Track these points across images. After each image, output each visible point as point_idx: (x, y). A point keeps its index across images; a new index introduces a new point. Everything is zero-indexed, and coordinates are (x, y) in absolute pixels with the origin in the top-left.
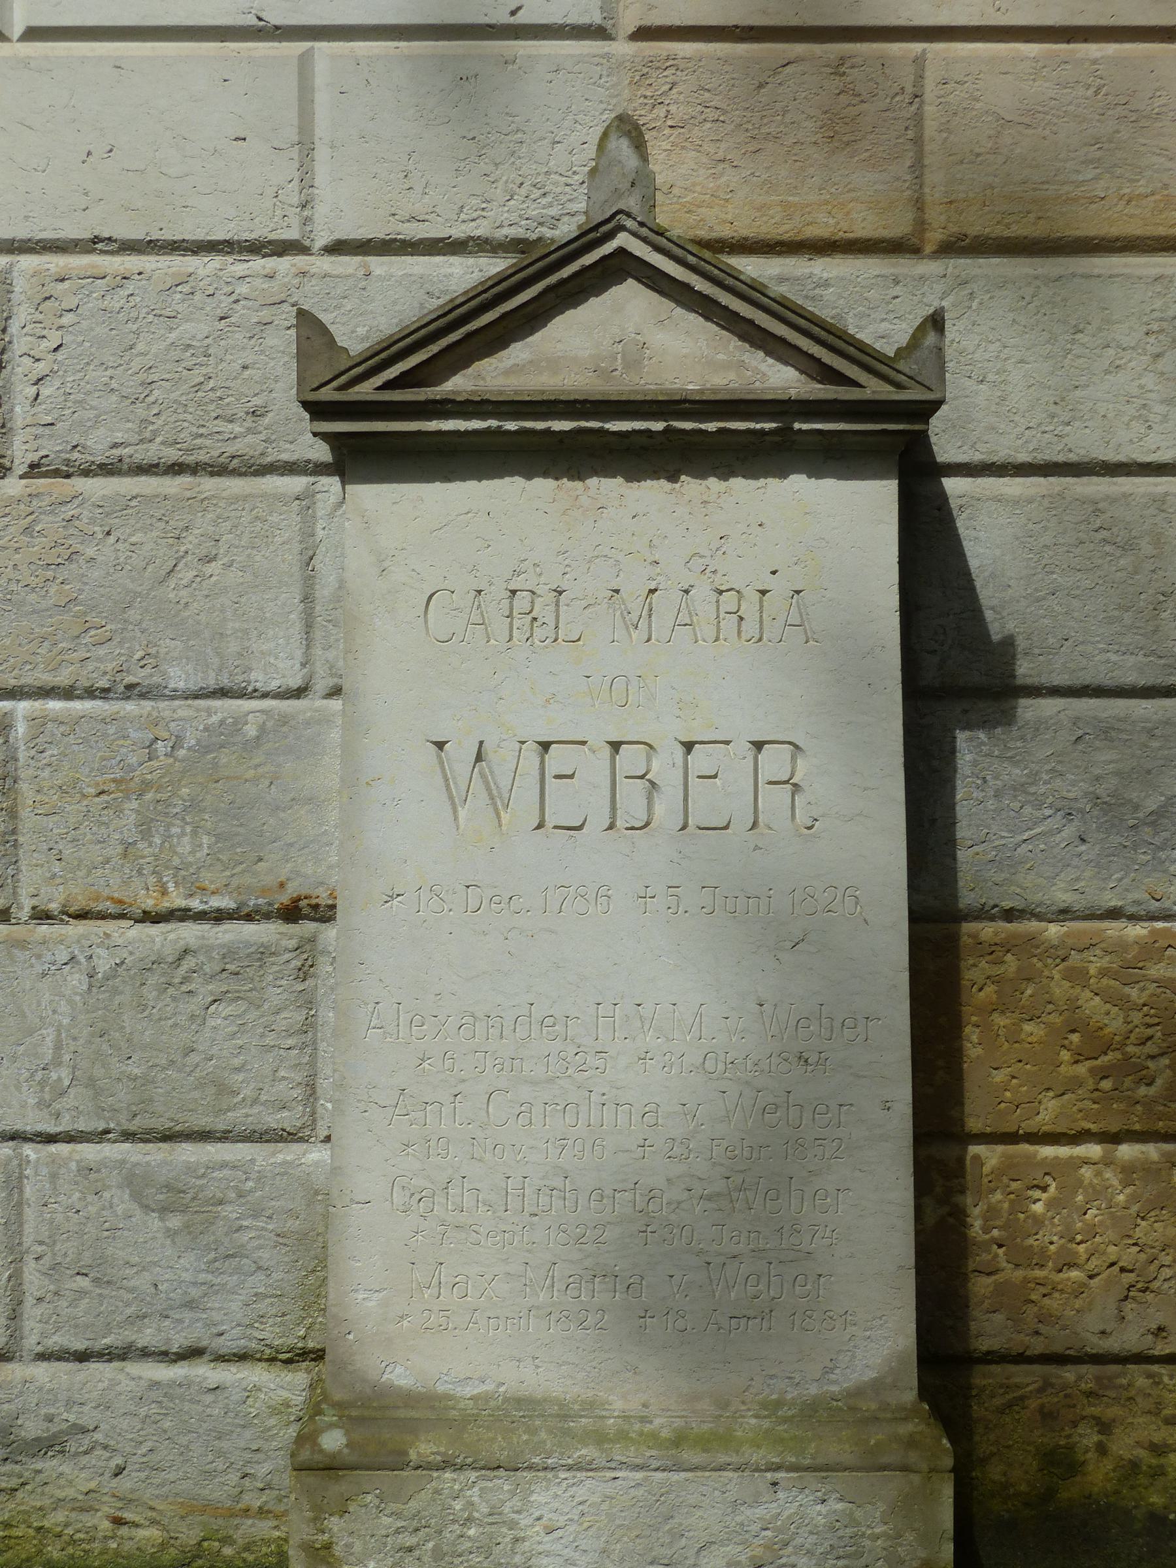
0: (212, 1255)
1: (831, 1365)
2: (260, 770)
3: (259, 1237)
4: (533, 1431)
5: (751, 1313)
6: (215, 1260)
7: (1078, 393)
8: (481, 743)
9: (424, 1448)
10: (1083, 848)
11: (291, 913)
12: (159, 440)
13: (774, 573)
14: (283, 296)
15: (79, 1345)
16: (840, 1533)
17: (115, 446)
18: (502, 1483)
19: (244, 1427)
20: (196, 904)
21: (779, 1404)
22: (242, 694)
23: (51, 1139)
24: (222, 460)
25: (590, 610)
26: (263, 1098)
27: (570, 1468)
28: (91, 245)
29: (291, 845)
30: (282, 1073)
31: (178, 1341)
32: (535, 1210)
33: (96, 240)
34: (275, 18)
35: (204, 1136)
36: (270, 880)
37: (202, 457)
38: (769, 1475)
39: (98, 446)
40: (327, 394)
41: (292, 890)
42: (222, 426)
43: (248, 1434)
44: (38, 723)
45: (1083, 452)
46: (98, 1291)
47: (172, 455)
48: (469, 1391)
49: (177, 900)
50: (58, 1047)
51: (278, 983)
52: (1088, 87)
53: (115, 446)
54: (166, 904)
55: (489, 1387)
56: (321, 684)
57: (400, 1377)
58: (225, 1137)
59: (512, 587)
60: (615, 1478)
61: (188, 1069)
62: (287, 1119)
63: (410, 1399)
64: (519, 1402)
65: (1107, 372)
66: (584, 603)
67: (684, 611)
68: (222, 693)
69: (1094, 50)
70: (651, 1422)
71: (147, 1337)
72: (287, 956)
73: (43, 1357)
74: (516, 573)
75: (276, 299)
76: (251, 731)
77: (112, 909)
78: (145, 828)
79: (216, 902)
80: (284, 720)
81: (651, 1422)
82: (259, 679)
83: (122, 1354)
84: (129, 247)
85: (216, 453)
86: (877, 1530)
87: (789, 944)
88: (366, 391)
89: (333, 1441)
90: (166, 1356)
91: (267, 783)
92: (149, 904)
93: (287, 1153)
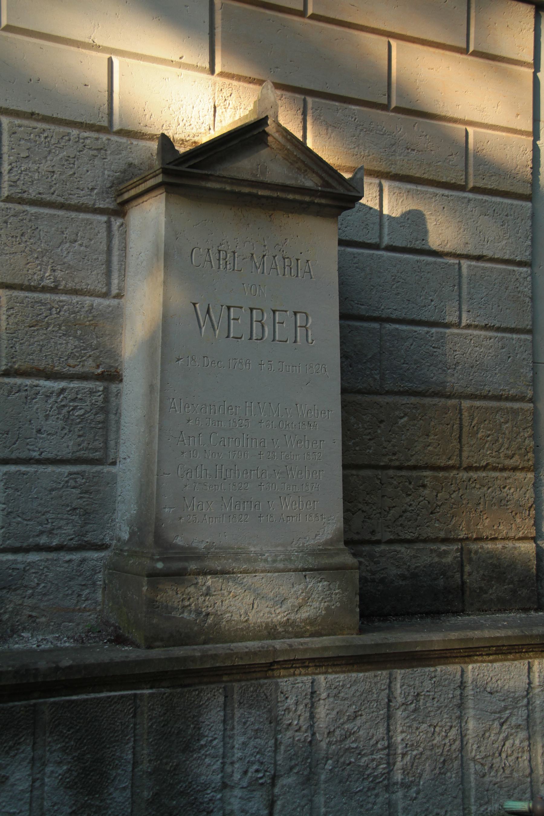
0: (69, 509)
1: (318, 533)
2: (91, 322)
3: (87, 501)
5: (293, 515)
6: (70, 510)
7: (349, 218)
8: (209, 305)
10: (350, 369)
11: (100, 377)
12: (56, 194)
13: (301, 253)
14: (102, 147)
15: (18, 545)
16: (326, 593)
17: (40, 194)
19: (79, 576)
24: (79, 204)
25: (245, 260)
26: (90, 447)
27: (241, 573)
29: (101, 351)
30: (97, 438)
31: (55, 542)
32: (225, 477)
33: (33, 114)
38: (304, 573)
39: (32, 194)
40: (171, 167)
42: (79, 191)
43: (80, 578)
45: (350, 237)
46: (25, 522)
51: (97, 403)
52: (352, 118)
53: (40, 194)
57: (179, 541)
59: (220, 248)
60: (255, 576)
61: (62, 435)
62: (97, 455)
65: (357, 212)
66: (243, 257)
67: (274, 264)
70: (264, 555)
71: (43, 540)
72: (100, 393)
74: (221, 245)
75: (99, 147)
81: (264, 555)
85: (76, 201)
86: (337, 591)
87: (305, 383)
88: (183, 168)
91: (93, 327)
93: (99, 468)
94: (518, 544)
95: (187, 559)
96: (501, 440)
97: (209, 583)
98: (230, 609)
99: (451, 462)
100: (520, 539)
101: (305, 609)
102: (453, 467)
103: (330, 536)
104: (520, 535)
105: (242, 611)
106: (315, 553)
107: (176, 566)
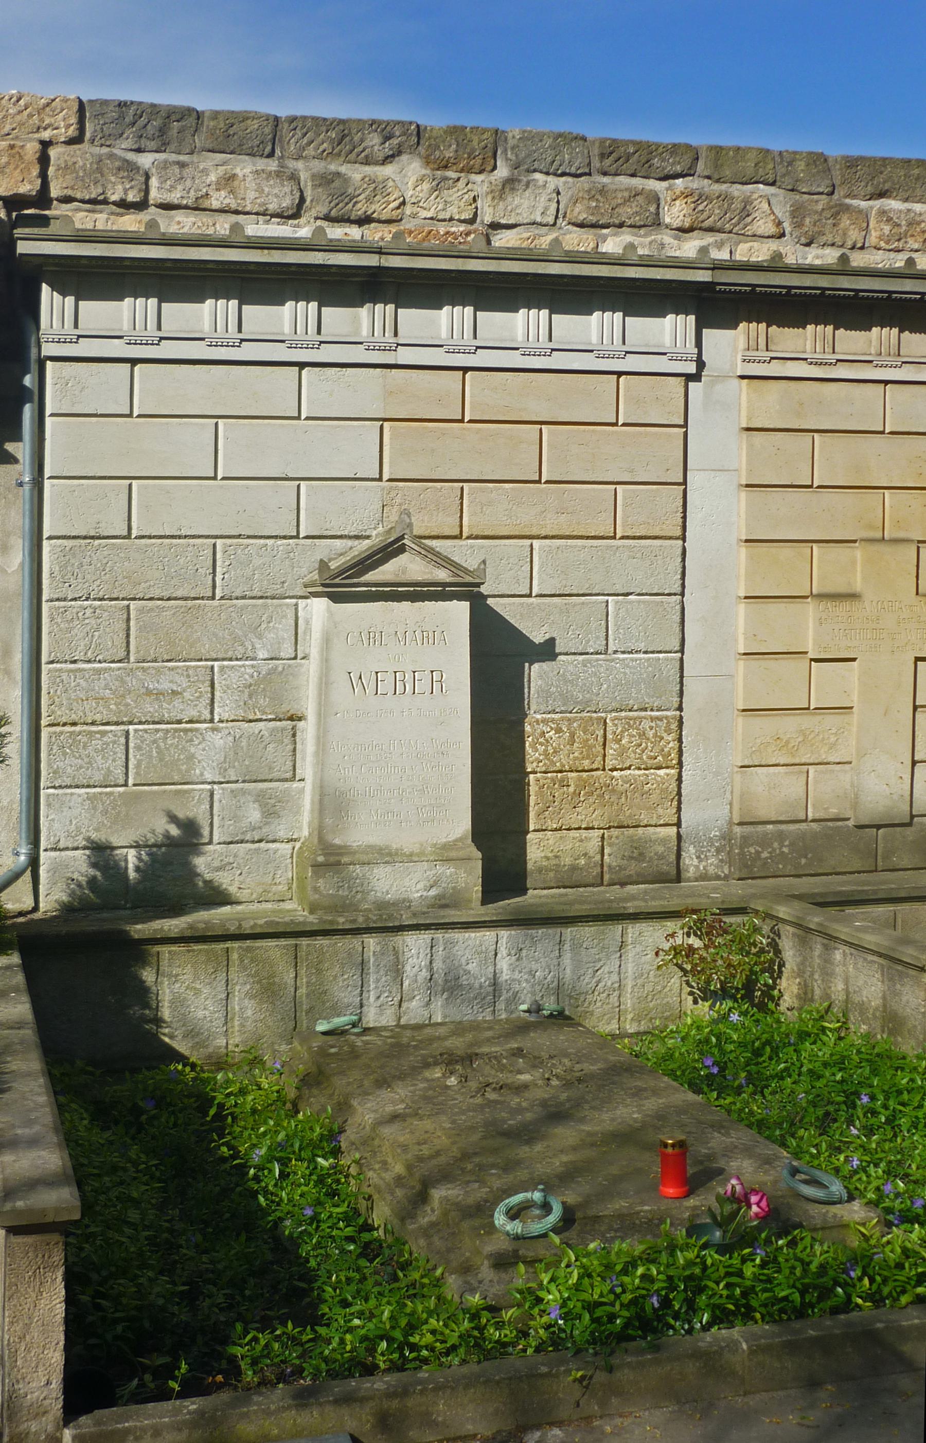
4: (373, 854)
9: (345, 859)
11: (291, 719)
18: (366, 868)
20: (264, 717)
21: (436, 844)
22: (278, 659)
23: (222, 783)
28: (239, 536)
34: (290, 476)
35: (265, 781)
36: (283, 710)
37: (269, 594)
41: (292, 712)
44: (222, 668)
47: (260, 594)
48: (355, 844)
49: (259, 716)
50: (225, 758)
54: (256, 717)
55: (361, 843)
56: (300, 656)
58: (271, 781)
62: (289, 775)
63: (340, 847)
64: (369, 846)
68: (272, 659)
69: (506, 485)
73: (219, 843)
76: (280, 669)
77: (241, 718)
78: (250, 696)
79: (270, 717)
80: (290, 666)
82: (282, 655)
83: (242, 842)
84: (249, 537)
89: (321, 859)
90: (253, 842)
92: (251, 717)
94: (659, 829)
95: (341, 854)
96: (644, 745)
97: (358, 870)
98: (375, 888)
99: (595, 766)
100: (661, 825)
101: (434, 889)
102: (597, 769)
103: (459, 836)
104: (662, 822)
105: (384, 890)
106: (445, 847)
107: (332, 859)
